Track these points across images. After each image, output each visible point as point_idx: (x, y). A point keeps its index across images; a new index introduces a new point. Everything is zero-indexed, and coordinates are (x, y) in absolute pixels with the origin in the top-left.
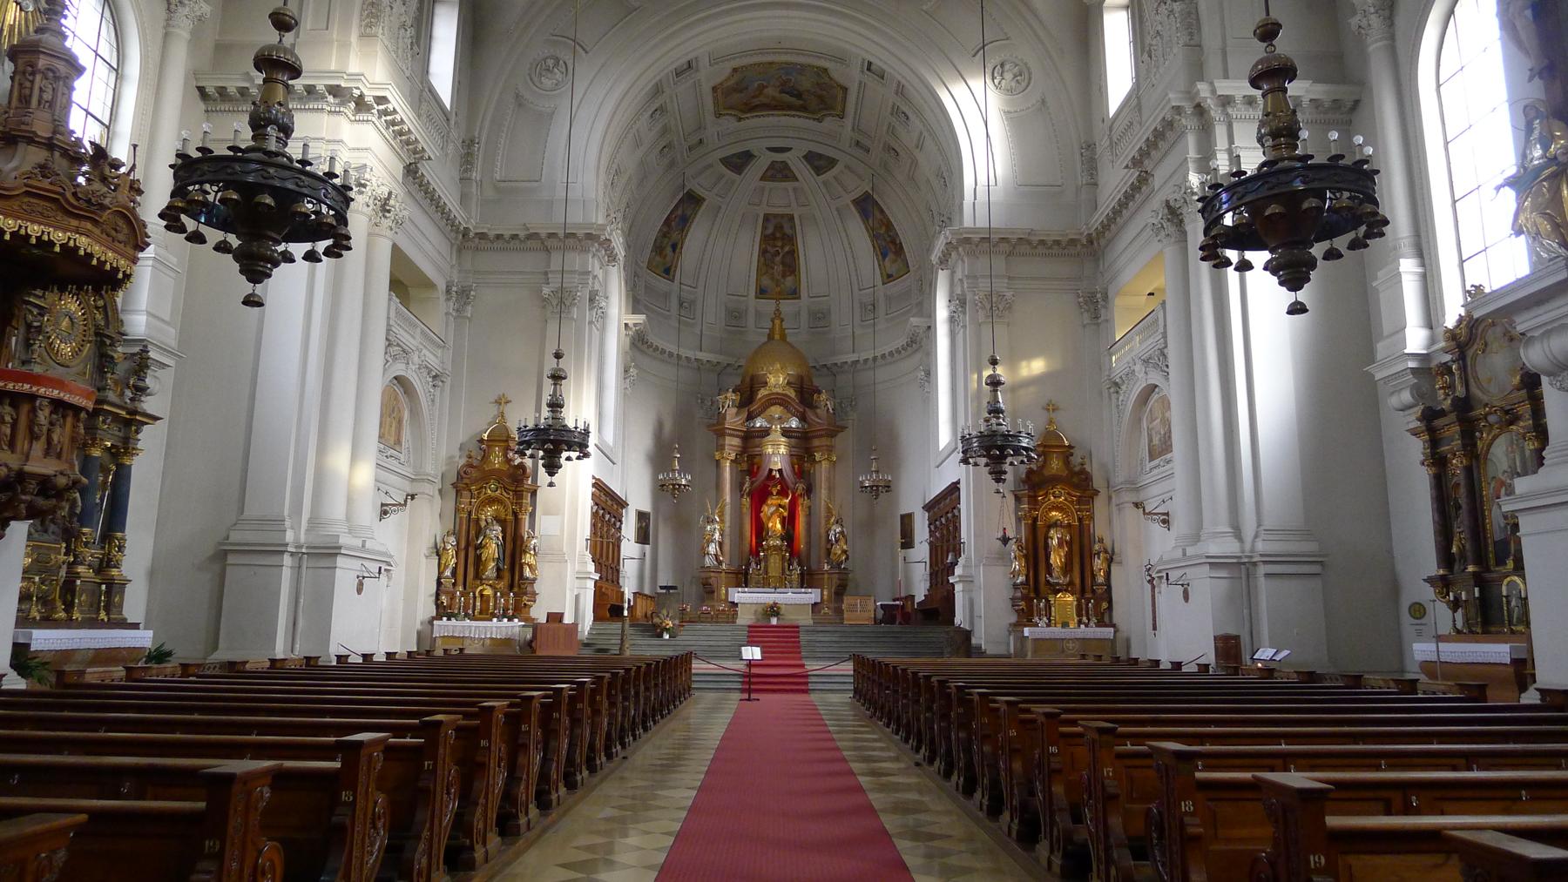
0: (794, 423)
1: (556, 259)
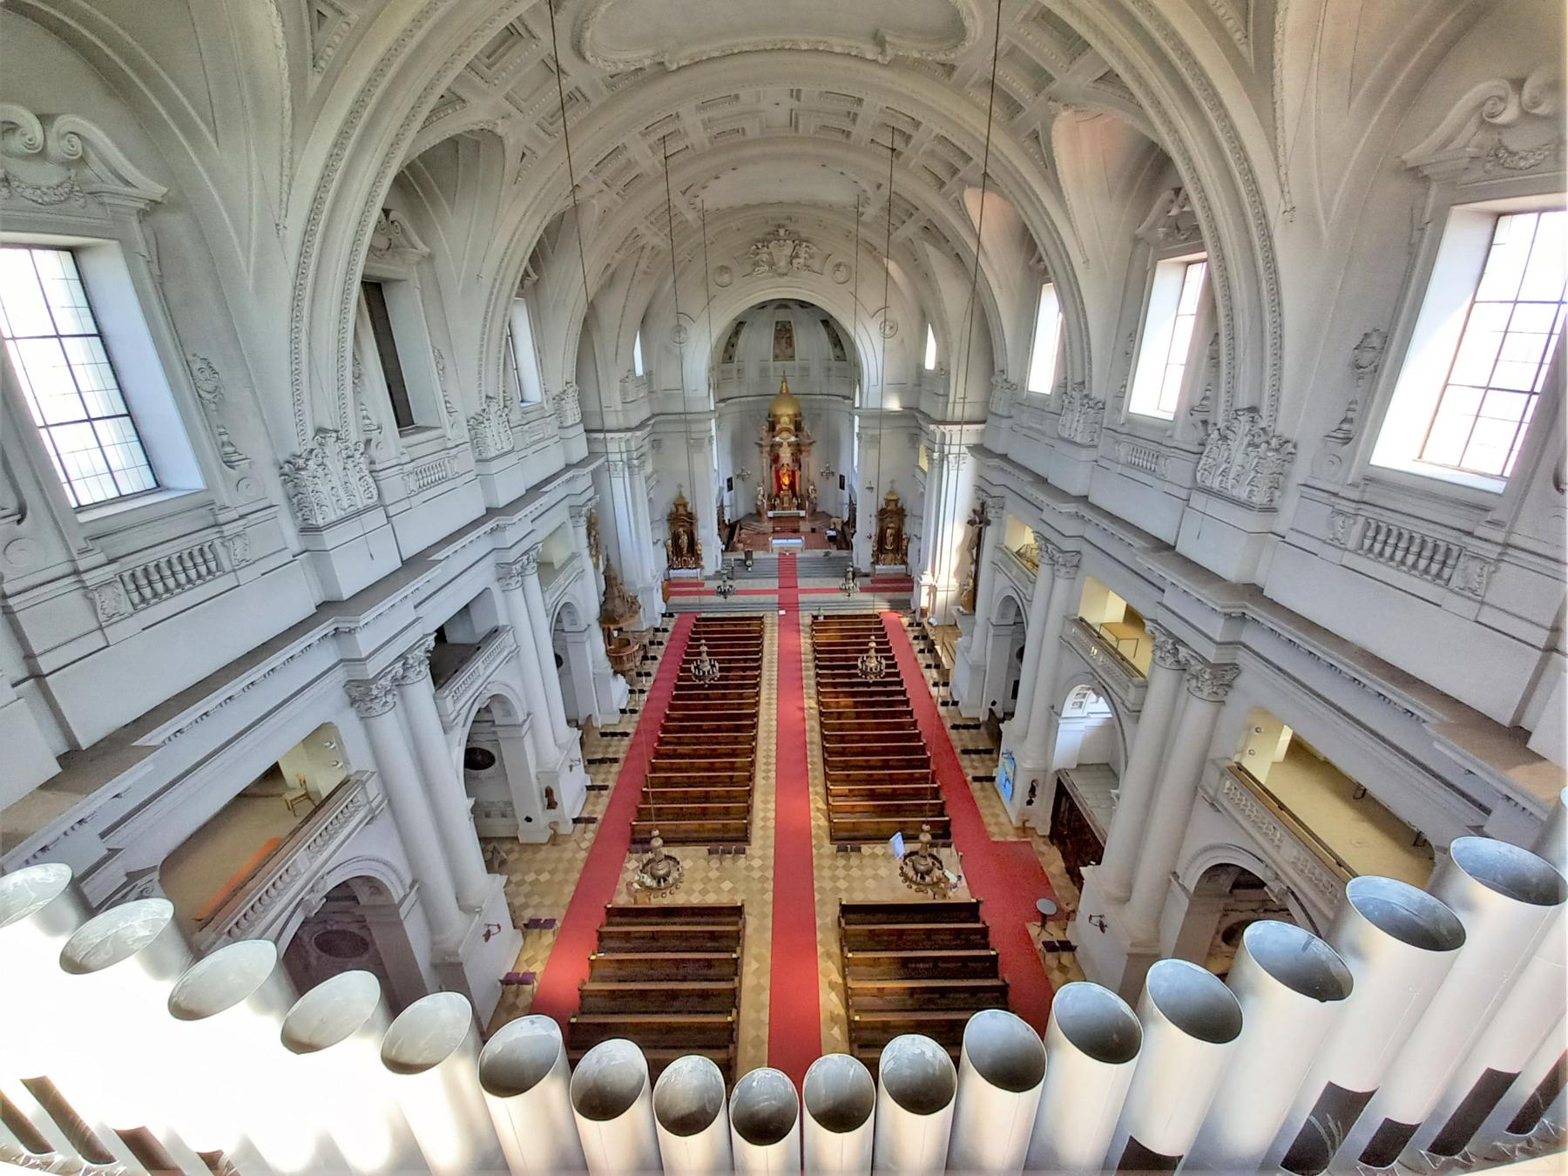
0: (793, 439)
1: (694, 427)
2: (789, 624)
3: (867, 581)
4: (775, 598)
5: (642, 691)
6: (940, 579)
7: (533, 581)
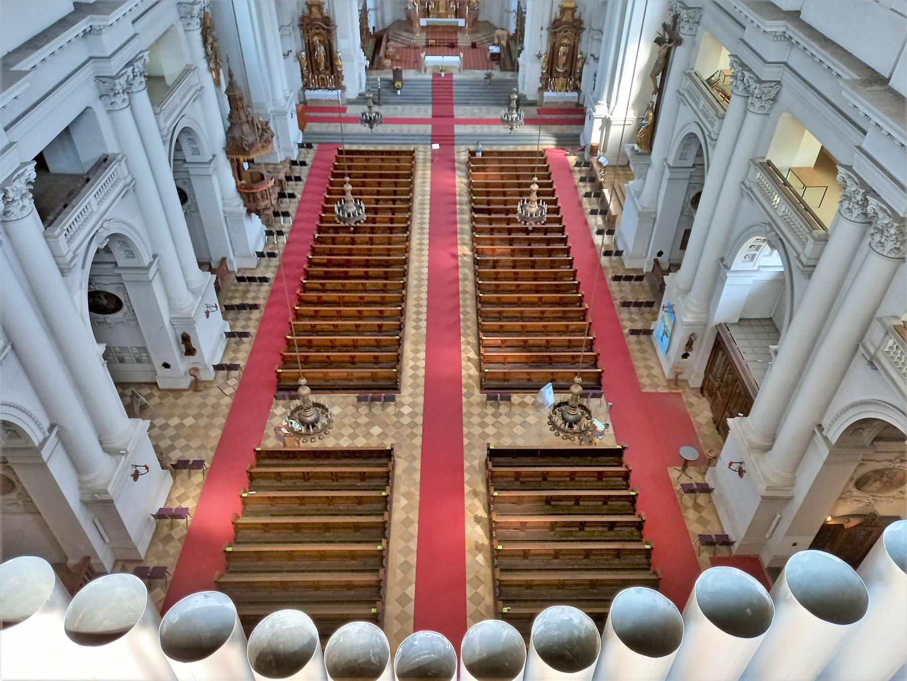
2: (443, 162)
3: (533, 111)
4: (428, 129)
5: (280, 233)
6: (615, 113)
7: (142, 99)
